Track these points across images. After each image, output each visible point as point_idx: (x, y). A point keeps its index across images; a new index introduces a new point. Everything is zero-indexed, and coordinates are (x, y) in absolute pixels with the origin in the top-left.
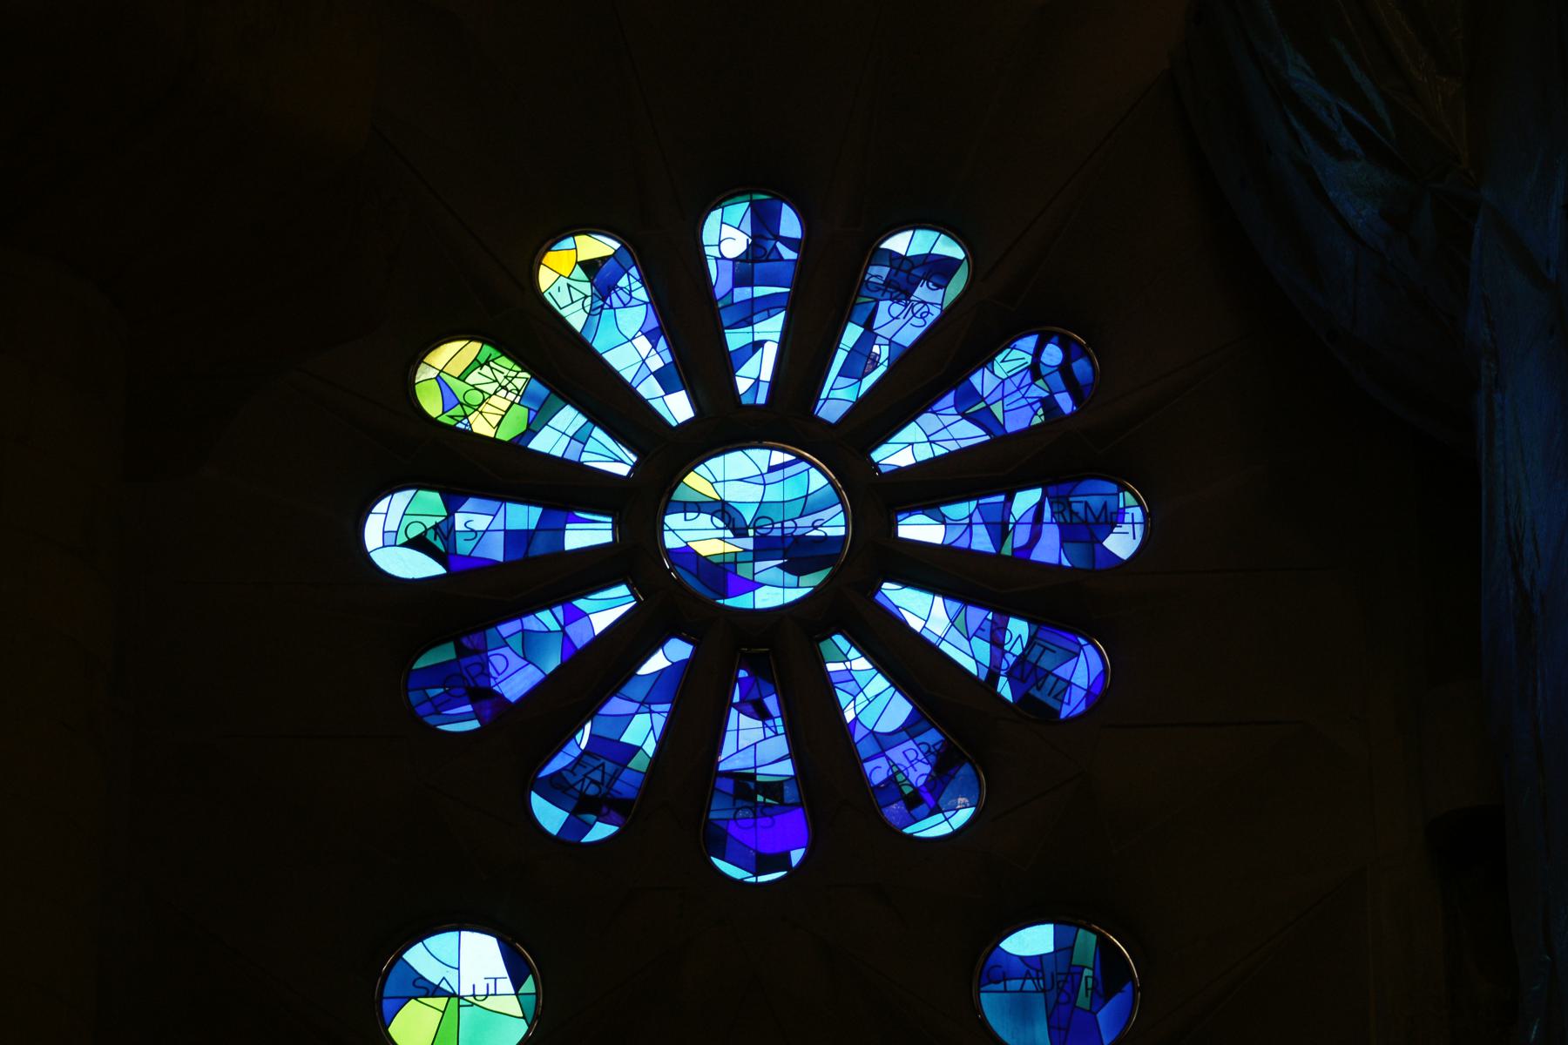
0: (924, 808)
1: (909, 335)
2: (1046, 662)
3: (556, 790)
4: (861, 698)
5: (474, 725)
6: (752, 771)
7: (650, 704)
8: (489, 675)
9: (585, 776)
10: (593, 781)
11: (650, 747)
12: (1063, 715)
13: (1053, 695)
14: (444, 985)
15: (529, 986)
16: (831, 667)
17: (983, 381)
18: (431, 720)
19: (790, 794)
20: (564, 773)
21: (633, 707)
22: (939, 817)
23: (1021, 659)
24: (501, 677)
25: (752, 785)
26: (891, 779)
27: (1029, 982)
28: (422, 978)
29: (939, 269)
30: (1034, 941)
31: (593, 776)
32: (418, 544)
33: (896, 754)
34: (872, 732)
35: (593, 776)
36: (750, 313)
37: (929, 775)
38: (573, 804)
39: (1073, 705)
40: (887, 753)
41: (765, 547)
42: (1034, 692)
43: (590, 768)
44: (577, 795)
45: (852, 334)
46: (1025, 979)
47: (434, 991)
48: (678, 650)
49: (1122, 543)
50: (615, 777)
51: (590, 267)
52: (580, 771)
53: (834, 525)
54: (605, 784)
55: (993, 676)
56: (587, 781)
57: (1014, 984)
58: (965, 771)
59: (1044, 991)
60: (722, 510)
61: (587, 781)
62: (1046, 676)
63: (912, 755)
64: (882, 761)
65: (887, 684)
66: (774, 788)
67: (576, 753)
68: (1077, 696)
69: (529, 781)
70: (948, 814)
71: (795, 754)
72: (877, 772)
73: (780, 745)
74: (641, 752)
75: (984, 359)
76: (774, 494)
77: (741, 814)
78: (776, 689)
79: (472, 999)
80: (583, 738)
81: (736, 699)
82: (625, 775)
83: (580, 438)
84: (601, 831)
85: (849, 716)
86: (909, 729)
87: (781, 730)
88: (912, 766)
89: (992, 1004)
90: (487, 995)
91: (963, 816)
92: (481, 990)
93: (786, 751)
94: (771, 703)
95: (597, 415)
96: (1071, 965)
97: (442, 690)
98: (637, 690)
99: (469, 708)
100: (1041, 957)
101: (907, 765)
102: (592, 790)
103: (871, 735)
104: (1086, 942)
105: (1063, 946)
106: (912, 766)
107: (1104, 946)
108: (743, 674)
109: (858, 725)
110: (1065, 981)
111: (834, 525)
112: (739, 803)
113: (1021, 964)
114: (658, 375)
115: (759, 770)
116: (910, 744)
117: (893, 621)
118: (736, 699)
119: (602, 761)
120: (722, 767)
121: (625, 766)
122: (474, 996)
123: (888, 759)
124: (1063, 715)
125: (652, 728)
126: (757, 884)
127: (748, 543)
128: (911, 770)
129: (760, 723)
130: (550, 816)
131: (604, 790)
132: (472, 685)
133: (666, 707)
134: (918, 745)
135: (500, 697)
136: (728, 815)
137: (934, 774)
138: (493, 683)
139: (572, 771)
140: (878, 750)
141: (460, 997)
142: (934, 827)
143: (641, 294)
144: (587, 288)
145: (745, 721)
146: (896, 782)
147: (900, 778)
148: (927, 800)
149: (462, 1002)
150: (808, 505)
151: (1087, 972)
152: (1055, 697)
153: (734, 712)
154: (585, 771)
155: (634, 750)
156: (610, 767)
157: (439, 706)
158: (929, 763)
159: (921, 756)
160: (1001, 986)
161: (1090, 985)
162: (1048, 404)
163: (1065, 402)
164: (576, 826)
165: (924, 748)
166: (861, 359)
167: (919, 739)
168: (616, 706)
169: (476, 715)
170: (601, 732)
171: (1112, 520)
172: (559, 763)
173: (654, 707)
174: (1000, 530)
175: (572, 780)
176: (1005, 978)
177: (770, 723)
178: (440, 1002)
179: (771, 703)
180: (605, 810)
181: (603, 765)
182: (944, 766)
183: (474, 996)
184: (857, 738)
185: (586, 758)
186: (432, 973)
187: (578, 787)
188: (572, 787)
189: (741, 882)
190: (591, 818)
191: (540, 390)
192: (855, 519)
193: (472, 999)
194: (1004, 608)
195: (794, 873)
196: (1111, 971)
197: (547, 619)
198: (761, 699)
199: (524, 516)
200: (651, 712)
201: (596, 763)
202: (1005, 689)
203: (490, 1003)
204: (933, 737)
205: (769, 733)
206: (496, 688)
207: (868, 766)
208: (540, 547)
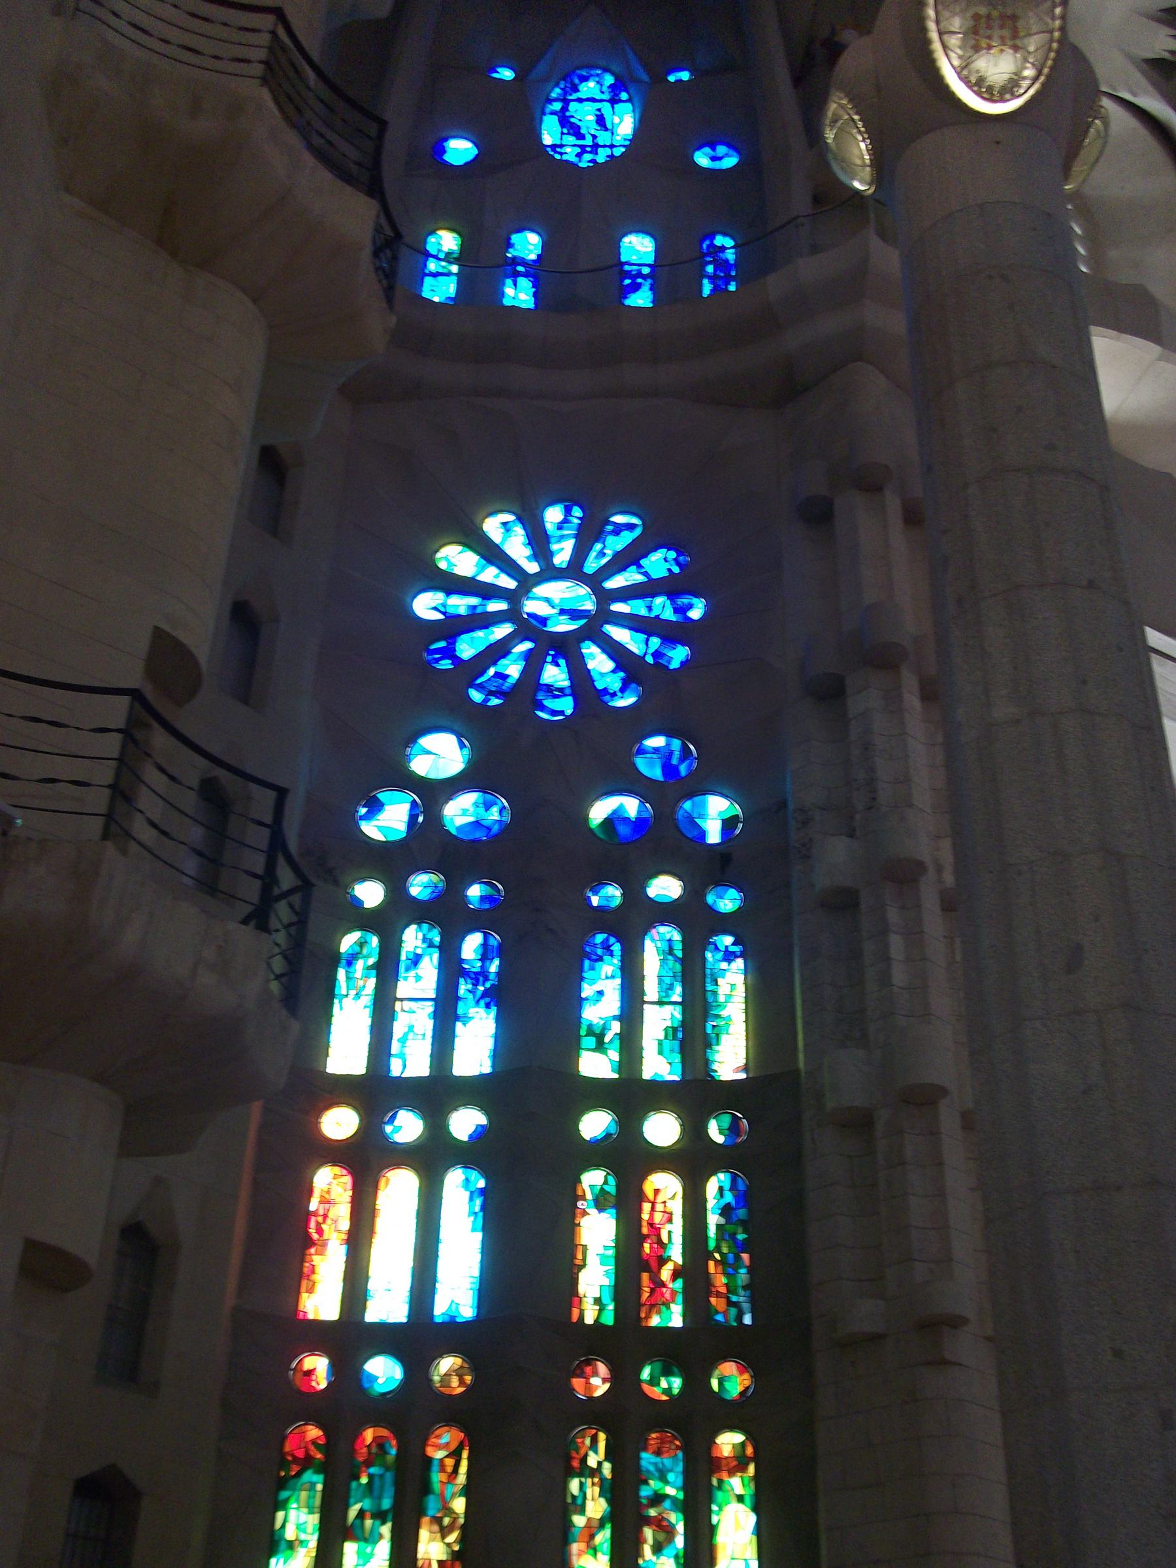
1: (619, 547)
2: (665, 651)
3: (480, 688)
16: (583, 651)
17: (643, 562)
19: (568, 691)
21: (509, 662)
23: (656, 651)
29: (630, 527)
32: (435, 609)
36: (562, 537)
39: (675, 665)
41: (563, 612)
45: (598, 547)
48: (528, 645)
49: (696, 614)
50: (502, 685)
51: (505, 524)
53: (590, 605)
55: (646, 654)
57: (648, 755)
60: (547, 600)
66: (561, 690)
73: (565, 676)
75: (645, 556)
76: (567, 595)
80: (491, 671)
83: (497, 576)
84: (495, 701)
86: (613, 671)
95: (502, 570)
98: (510, 657)
102: (493, 689)
104: (676, 744)
105: (668, 745)
111: (590, 605)
114: (528, 558)
117: (609, 638)
127: (557, 611)
130: (476, 696)
143: (522, 532)
144: (503, 530)
150: (579, 598)
155: (507, 676)
162: (669, 570)
163: (676, 570)
166: (602, 554)
168: (503, 662)
171: (690, 606)
172: (479, 681)
174: (650, 608)
185: (492, 679)
191: (484, 562)
192: (598, 603)
194: (649, 634)
196: (685, 754)
197: (480, 634)
199: (474, 601)
202: (649, 659)
208: (479, 610)
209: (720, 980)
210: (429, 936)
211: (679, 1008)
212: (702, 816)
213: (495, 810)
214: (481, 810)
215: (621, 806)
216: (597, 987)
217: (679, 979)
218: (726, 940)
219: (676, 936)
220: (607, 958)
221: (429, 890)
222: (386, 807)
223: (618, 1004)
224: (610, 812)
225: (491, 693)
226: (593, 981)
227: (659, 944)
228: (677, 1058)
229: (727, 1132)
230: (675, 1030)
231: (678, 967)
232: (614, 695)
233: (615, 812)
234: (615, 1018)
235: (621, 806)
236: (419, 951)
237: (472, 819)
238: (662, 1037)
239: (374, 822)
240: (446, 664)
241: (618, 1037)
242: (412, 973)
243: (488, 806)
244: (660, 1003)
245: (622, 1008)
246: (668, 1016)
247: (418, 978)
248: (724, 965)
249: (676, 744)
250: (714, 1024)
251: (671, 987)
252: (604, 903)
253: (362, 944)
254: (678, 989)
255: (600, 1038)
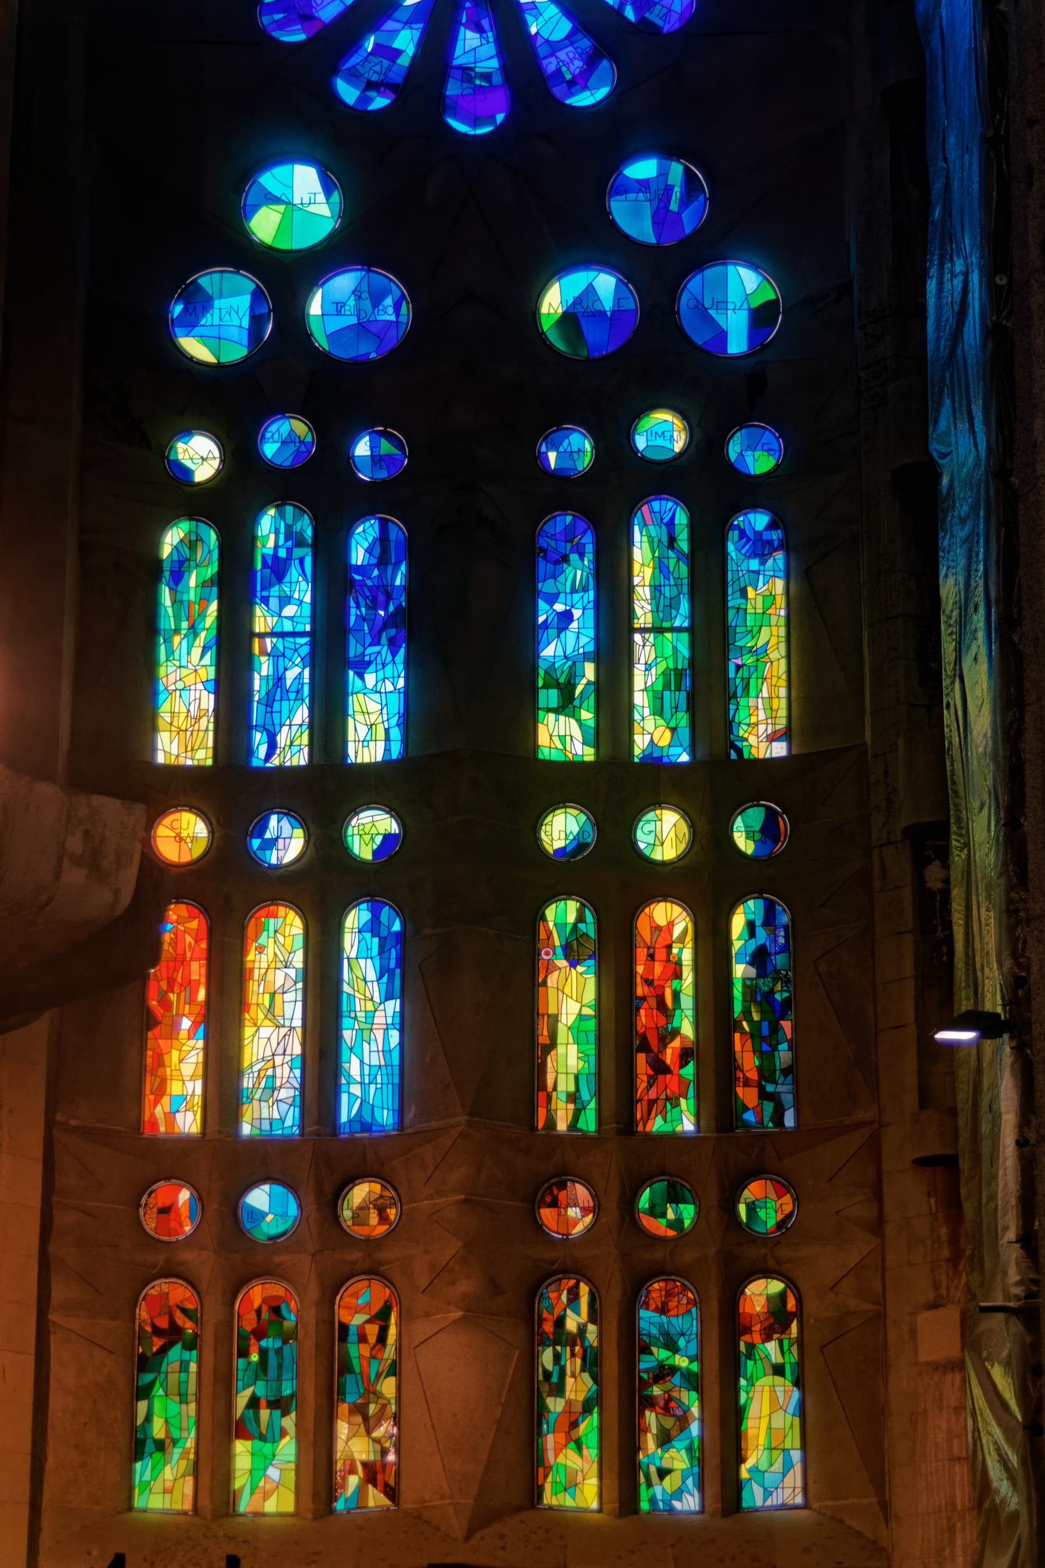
0: (578, 87)
3: (353, 76)
4: (541, 19)
5: (301, 37)
6: (473, 65)
7: (411, 23)
8: (312, 7)
9: (371, 68)
10: (375, 72)
11: (410, 50)
12: (665, 31)
13: (660, 15)
14: (283, 198)
15: (336, 197)
18: (275, 34)
19: (497, 79)
20: (357, 67)
21: (398, 25)
22: (588, 93)
24: (319, 8)
25: (473, 74)
26: (558, 70)
27: (641, 195)
28: (270, 193)
30: (643, 169)
31: (374, 68)
33: (562, 55)
34: (547, 41)
35: (374, 68)
37: (582, 67)
38: (364, 85)
40: (558, 54)
42: (647, 15)
43: (373, 64)
44: (365, 81)
46: (638, 193)
47: (277, 200)
52: (367, 65)
54: (383, 72)
56: (372, 72)
57: (632, 196)
58: (605, 64)
59: (650, 200)
61: (372, 72)
62: (655, 5)
63: (571, 55)
64: (553, 60)
65: (557, 11)
66: (487, 76)
67: (365, 55)
68: (675, 17)
69: (335, 71)
70: (593, 92)
71: (501, 53)
72: (550, 65)
73: (490, 49)
74: (404, 54)
77: (465, 92)
78: (488, 14)
79: (300, 206)
80: (370, 44)
81: (464, 20)
82: (395, 68)
84: (380, 102)
85: (533, 30)
87: (491, 39)
88: (571, 62)
89: (619, 209)
90: (310, 203)
91: (603, 92)
92: (306, 201)
93: (494, 52)
94: (485, 23)
96: (666, 185)
97: (281, 16)
99: (299, 27)
100: (648, 179)
101: (568, 60)
102: (374, 78)
103: (546, 43)
104: (676, 171)
105: (663, 174)
106: (571, 62)
107: (688, 174)
108: (468, 5)
109: (539, 37)
110: (663, 194)
112: (465, 85)
113: (637, 184)
115: (477, 65)
116: (570, 48)
118: (464, 20)
119: (381, 59)
120: (456, 62)
121: (394, 62)
122: (302, 204)
123: (557, 57)
124: (665, 31)
125: (412, 39)
126: (475, 136)
128: (571, 64)
129: (478, 36)
130: (348, 93)
131: (382, 77)
132: (301, 12)
133: (421, 26)
134: (575, 49)
135: (319, 19)
136: (458, 92)
137: (585, 67)
138: (314, 11)
139: (362, 66)
140: (551, 52)
141: (293, 205)
142: (584, 99)
145: (470, 34)
146: (561, 72)
147: (564, 69)
148: (581, 82)
149: (295, 208)
151: (677, 189)
152: (661, 18)
153: (462, 29)
154: (370, 66)
155: (399, 52)
156: (386, 63)
157: (281, 25)
158: (582, 60)
159: (577, 56)
160: (623, 197)
161: (678, 197)
164: (364, 99)
165: (579, 51)
167: (575, 45)
168: (390, 25)
169: (304, 30)
170: (381, 42)
172: (354, 61)
173: (413, 26)
175: (362, 71)
176: (626, 192)
177: (484, 35)
178: (281, 208)
179: (485, 23)
180: (382, 89)
181: (381, 62)
182: (591, 63)
183: (302, 204)
184: (538, 44)
185: (371, 58)
186: (276, 190)
187: (366, 75)
188: (362, 75)
189: (465, 135)
190: (372, 94)
193: (300, 206)
195: (499, 129)
198: (480, 20)
200: (412, 29)
201: (377, 61)
203: (312, 209)
204: (585, 43)
205: (484, 42)
206: (316, 14)
207: (545, 62)
209: (751, 592)
210: (297, 528)
211: (685, 637)
212: (722, 304)
213: (389, 301)
214: (367, 305)
215: (590, 289)
216: (559, 607)
217: (685, 589)
218: (760, 520)
219: (682, 518)
220: (574, 557)
221: (291, 449)
222: (217, 303)
223: (591, 633)
224: (570, 301)
225: (370, 85)
226: (552, 599)
227: (653, 530)
228: (683, 720)
229: (758, 836)
230: (679, 673)
231: (684, 570)
232: (572, 83)
233: (578, 300)
234: (586, 657)
235: (590, 289)
236: (282, 553)
237: (354, 320)
238: (659, 687)
239: (198, 330)
240: (296, 36)
241: (592, 687)
242: (274, 591)
243: (376, 300)
244: (658, 630)
245: (597, 639)
246: (668, 651)
247: (285, 600)
248: (754, 564)
249: (676, 171)
250: (739, 662)
251: (673, 604)
252: (567, 464)
253: (192, 542)
254: (685, 607)
255: (567, 691)
